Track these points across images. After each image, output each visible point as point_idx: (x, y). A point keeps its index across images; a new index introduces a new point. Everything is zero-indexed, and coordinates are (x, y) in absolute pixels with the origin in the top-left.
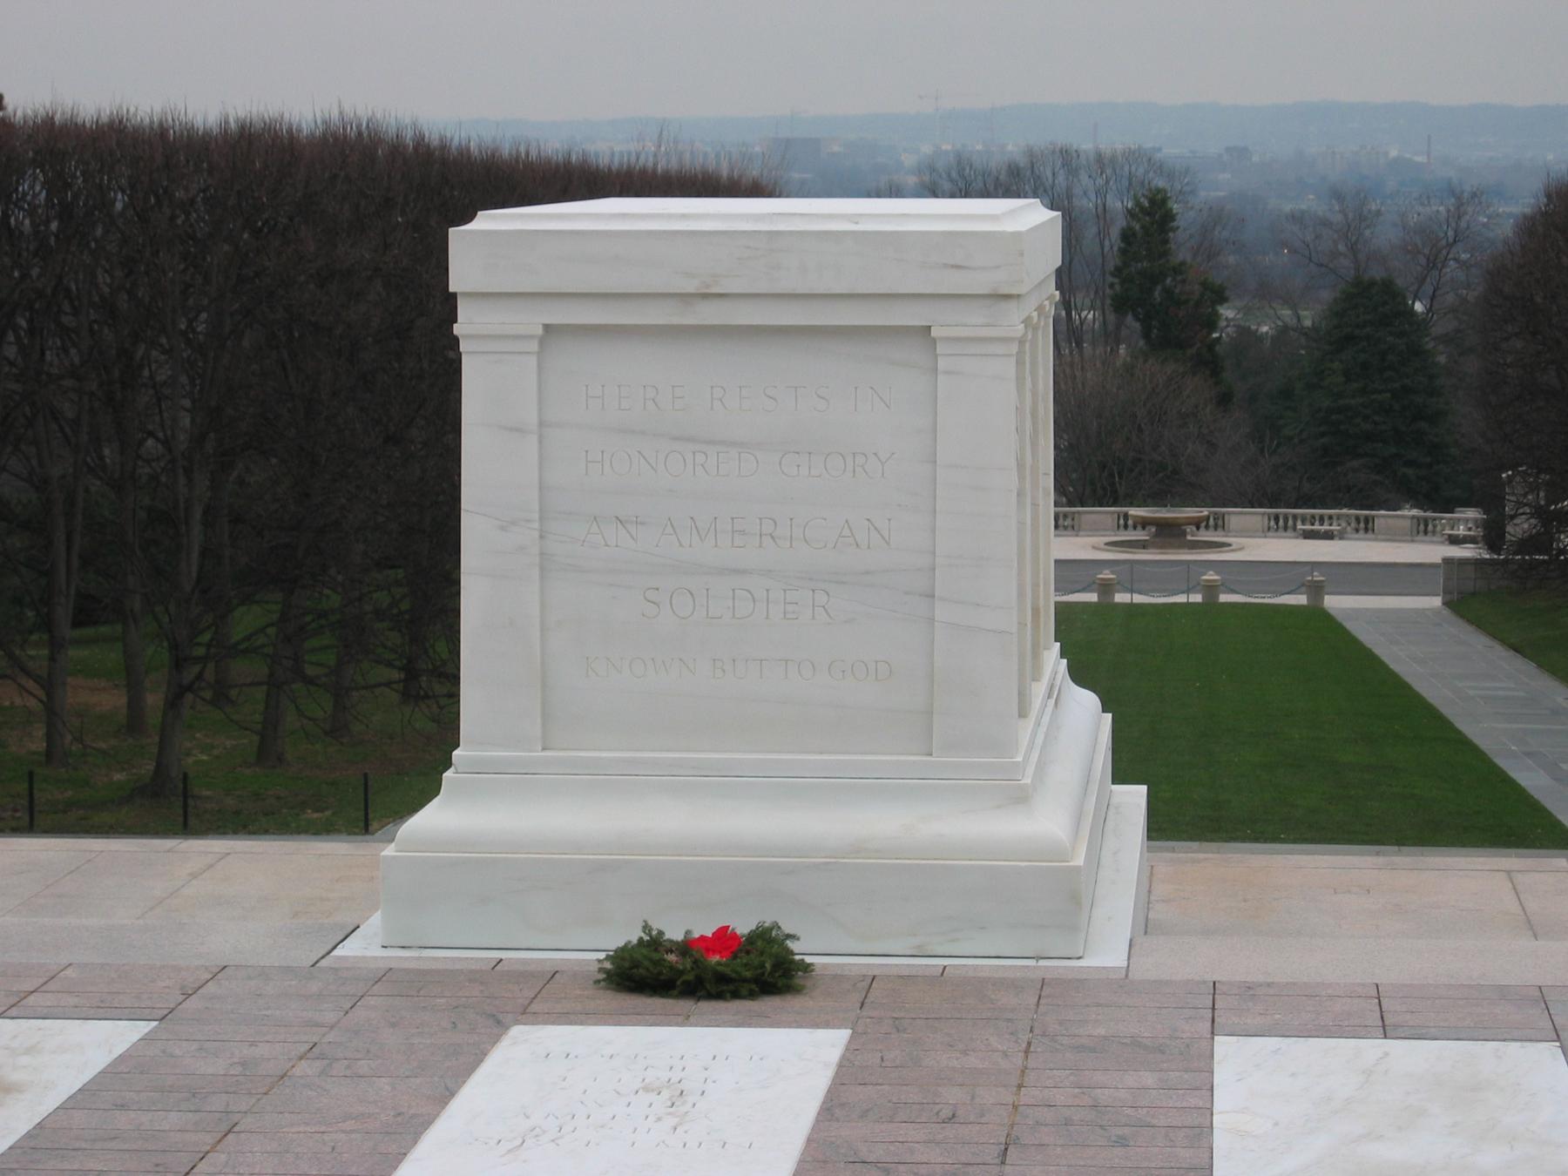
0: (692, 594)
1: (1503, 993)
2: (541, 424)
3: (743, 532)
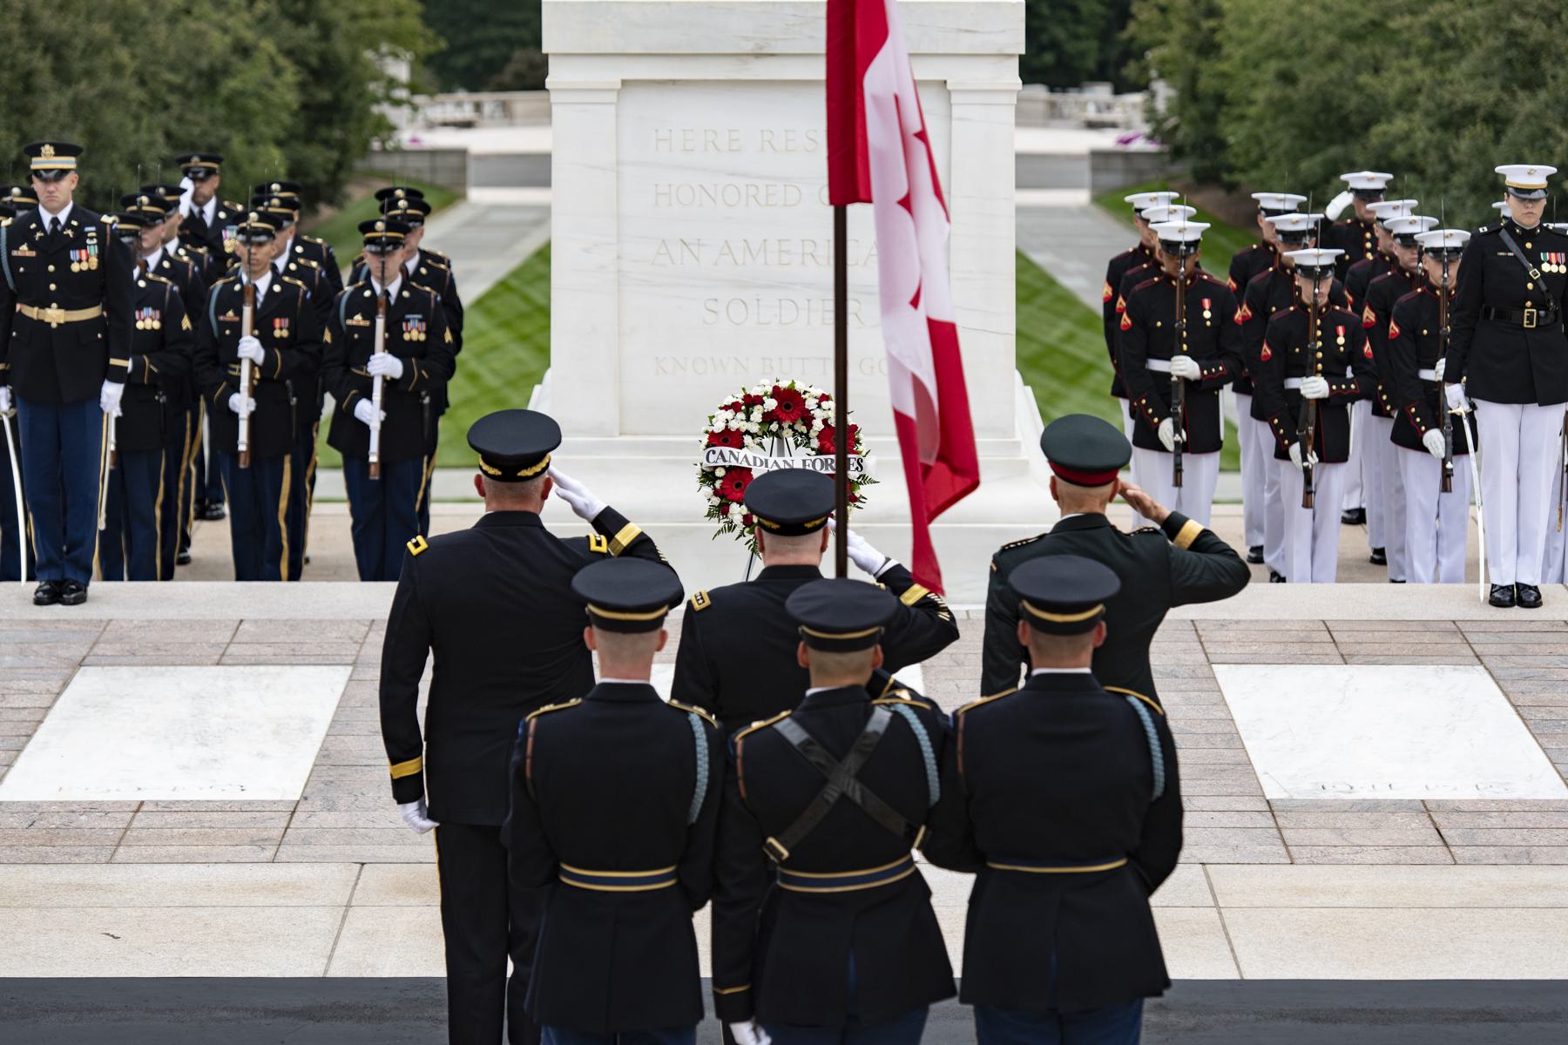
0: (744, 303)
1: (1426, 625)
2: (618, 163)
3: (787, 252)
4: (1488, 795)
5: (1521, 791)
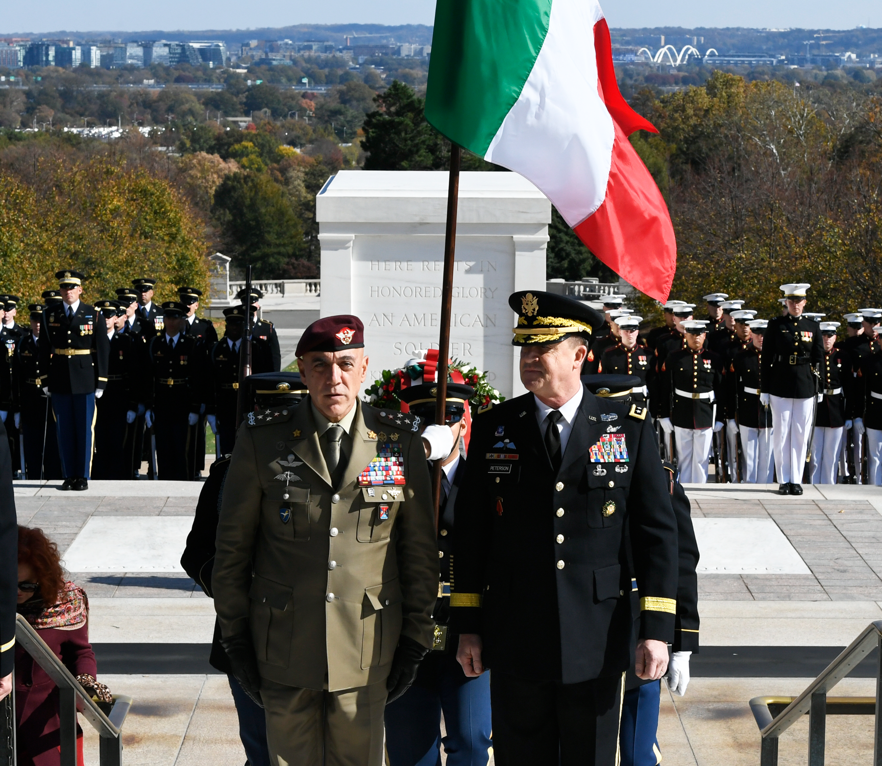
4: (771, 572)
5: (787, 570)
